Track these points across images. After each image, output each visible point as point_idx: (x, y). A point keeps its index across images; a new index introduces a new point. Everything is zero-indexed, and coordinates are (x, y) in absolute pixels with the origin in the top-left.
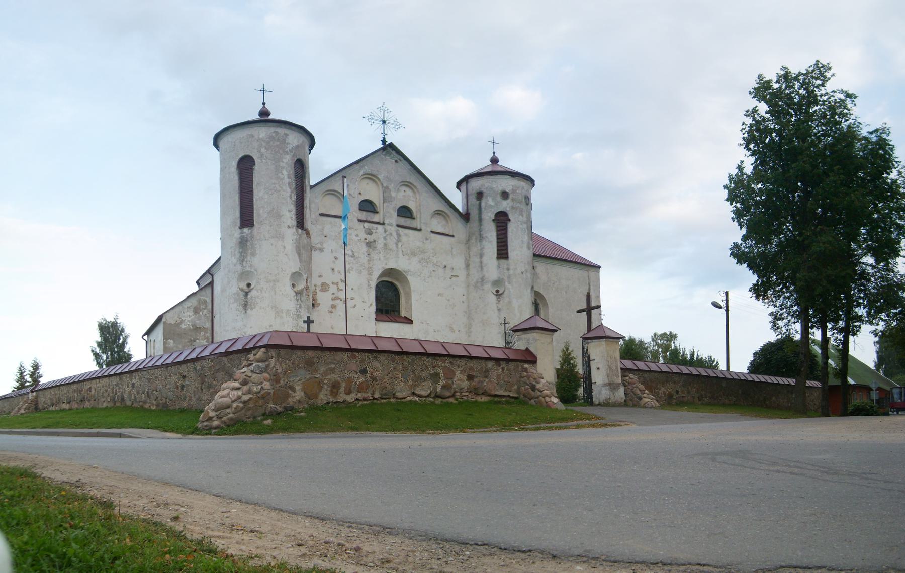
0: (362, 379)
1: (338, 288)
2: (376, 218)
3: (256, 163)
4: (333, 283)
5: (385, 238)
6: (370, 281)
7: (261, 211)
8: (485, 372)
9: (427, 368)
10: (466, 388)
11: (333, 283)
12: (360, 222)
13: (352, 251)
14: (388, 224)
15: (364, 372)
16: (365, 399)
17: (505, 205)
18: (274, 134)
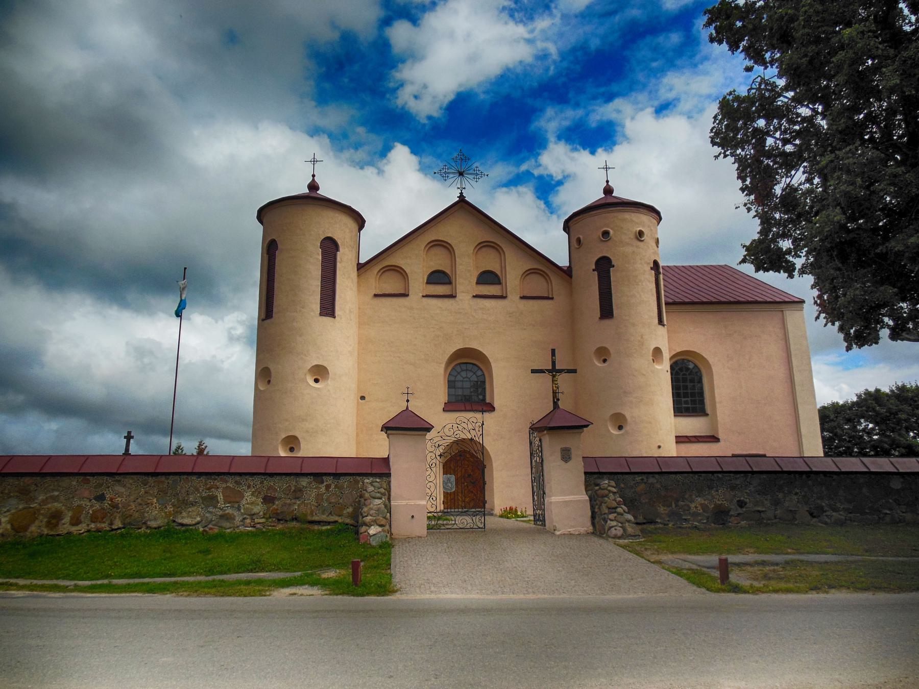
0: (97, 506)
8: (294, 491)
9: (197, 490)
10: (261, 513)
15: (101, 498)
16: (98, 531)
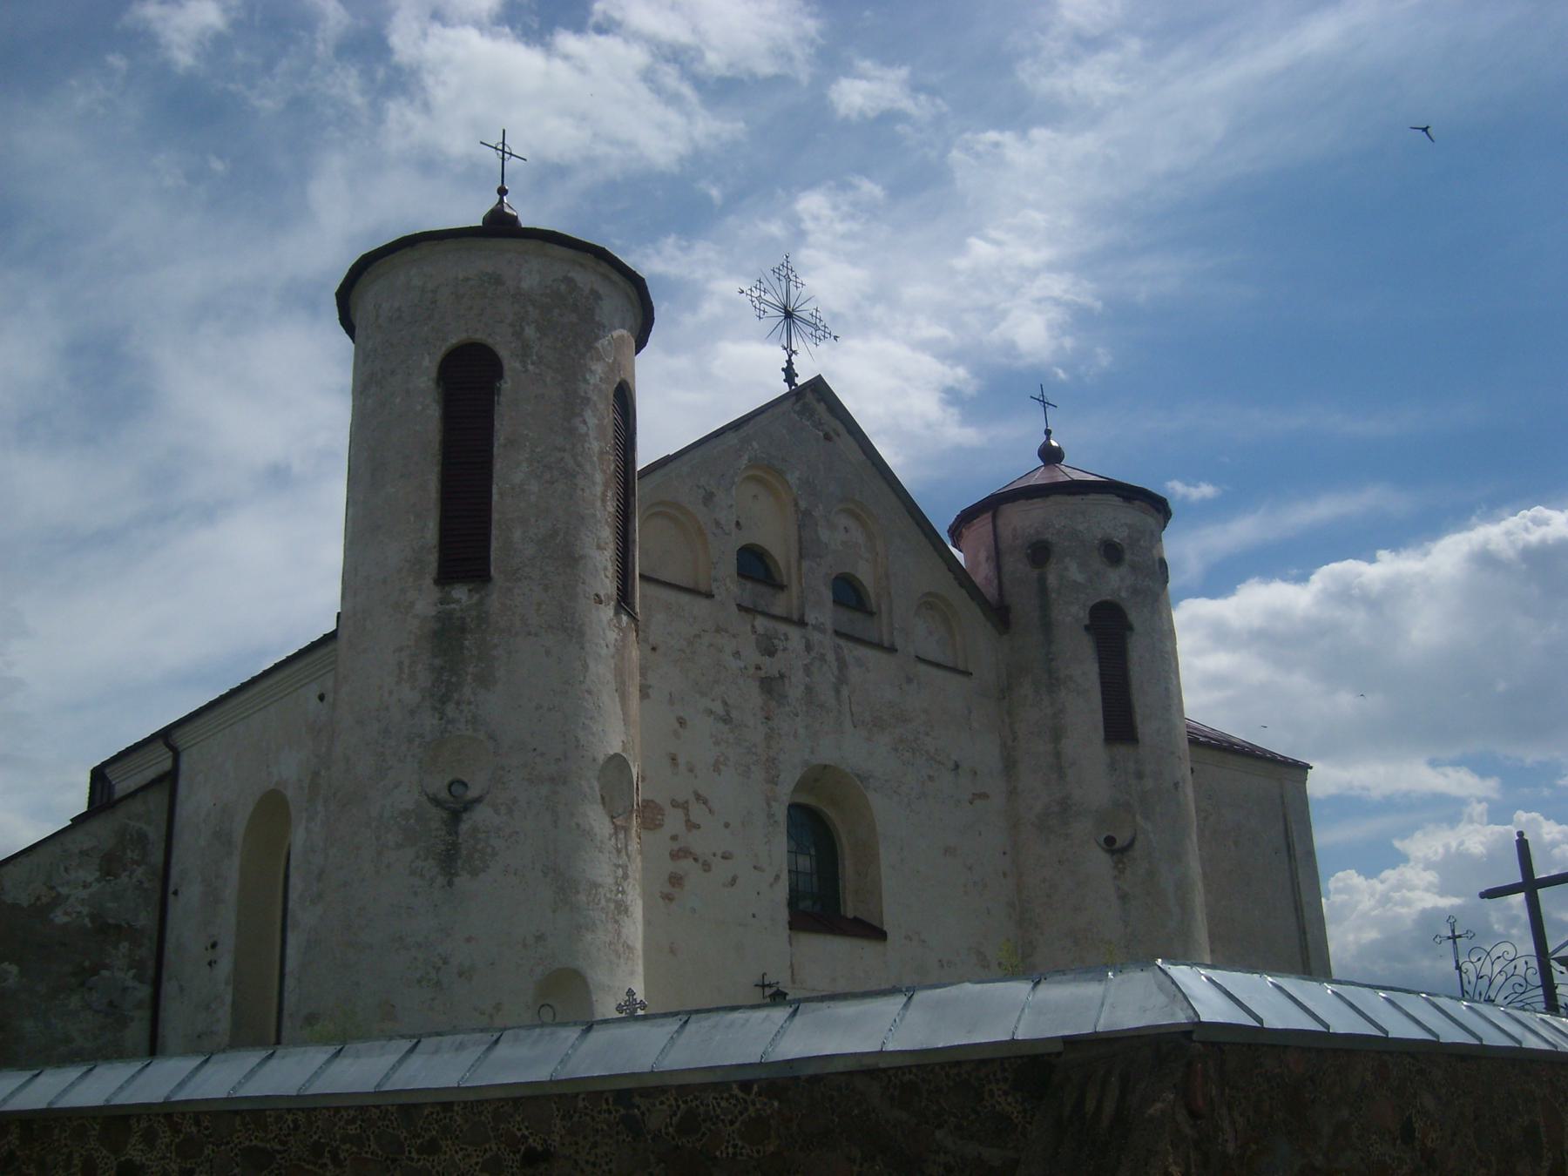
1: (688, 821)
2: (780, 605)
3: (507, 373)
4: (675, 804)
5: (807, 670)
6: (773, 804)
7: (517, 534)
11: (675, 804)
12: (743, 613)
13: (725, 703)
14: (814, 627)
17: (1115, 583)
18: (563, 287)
